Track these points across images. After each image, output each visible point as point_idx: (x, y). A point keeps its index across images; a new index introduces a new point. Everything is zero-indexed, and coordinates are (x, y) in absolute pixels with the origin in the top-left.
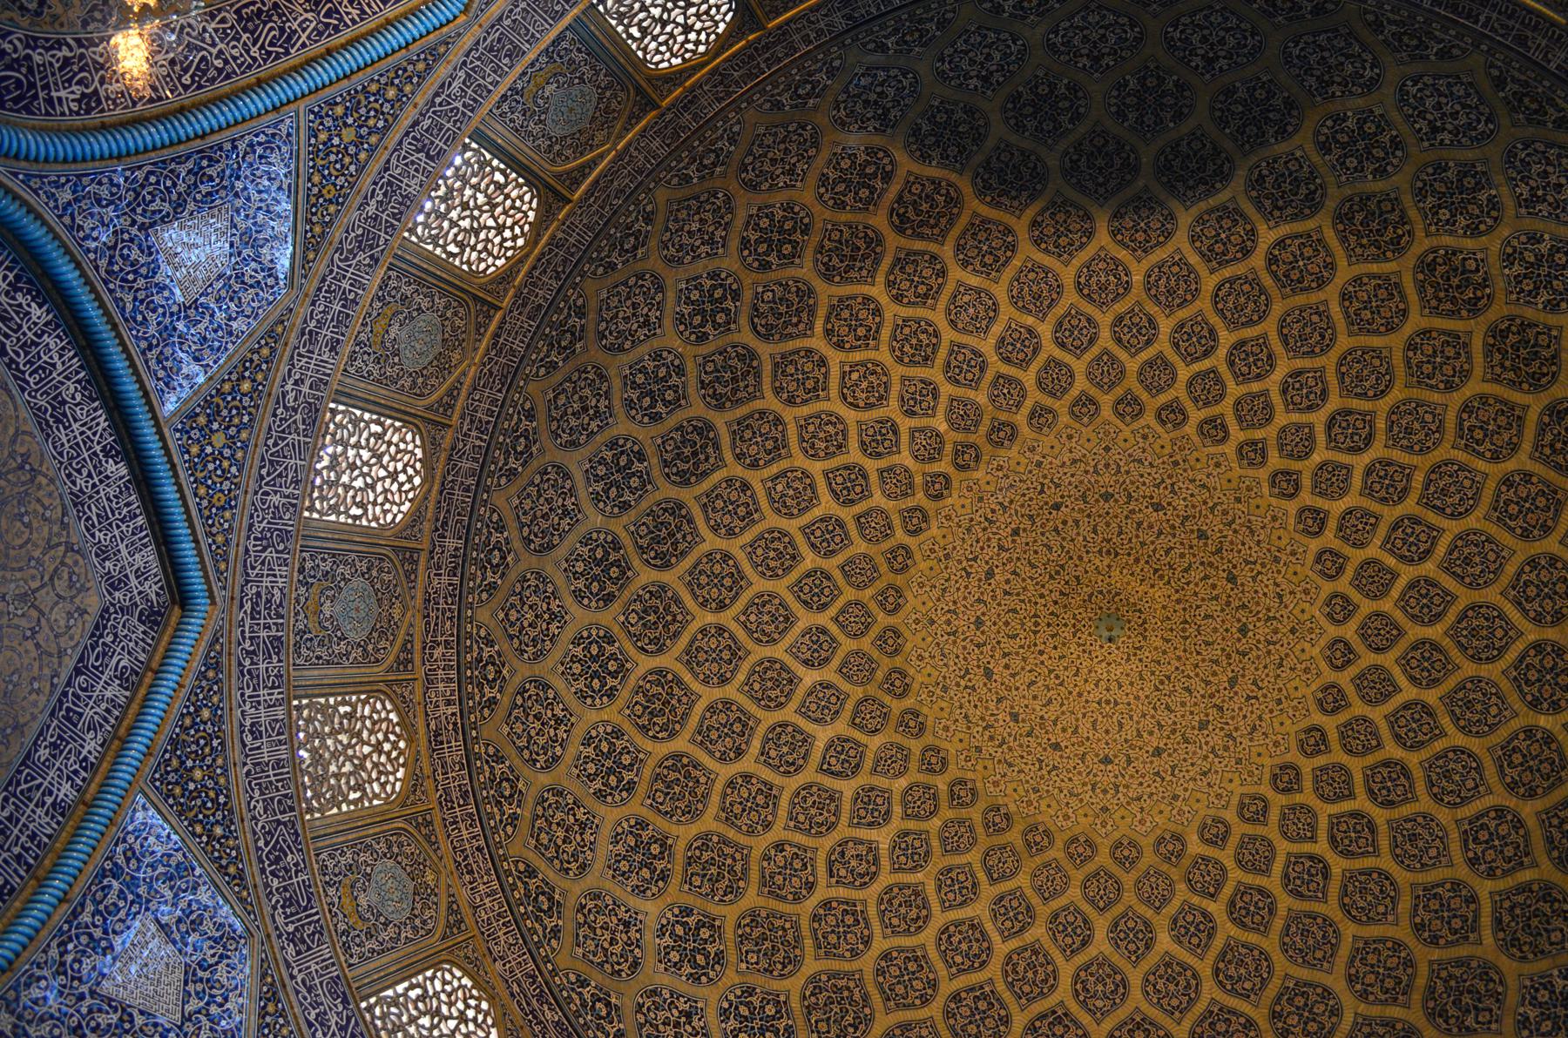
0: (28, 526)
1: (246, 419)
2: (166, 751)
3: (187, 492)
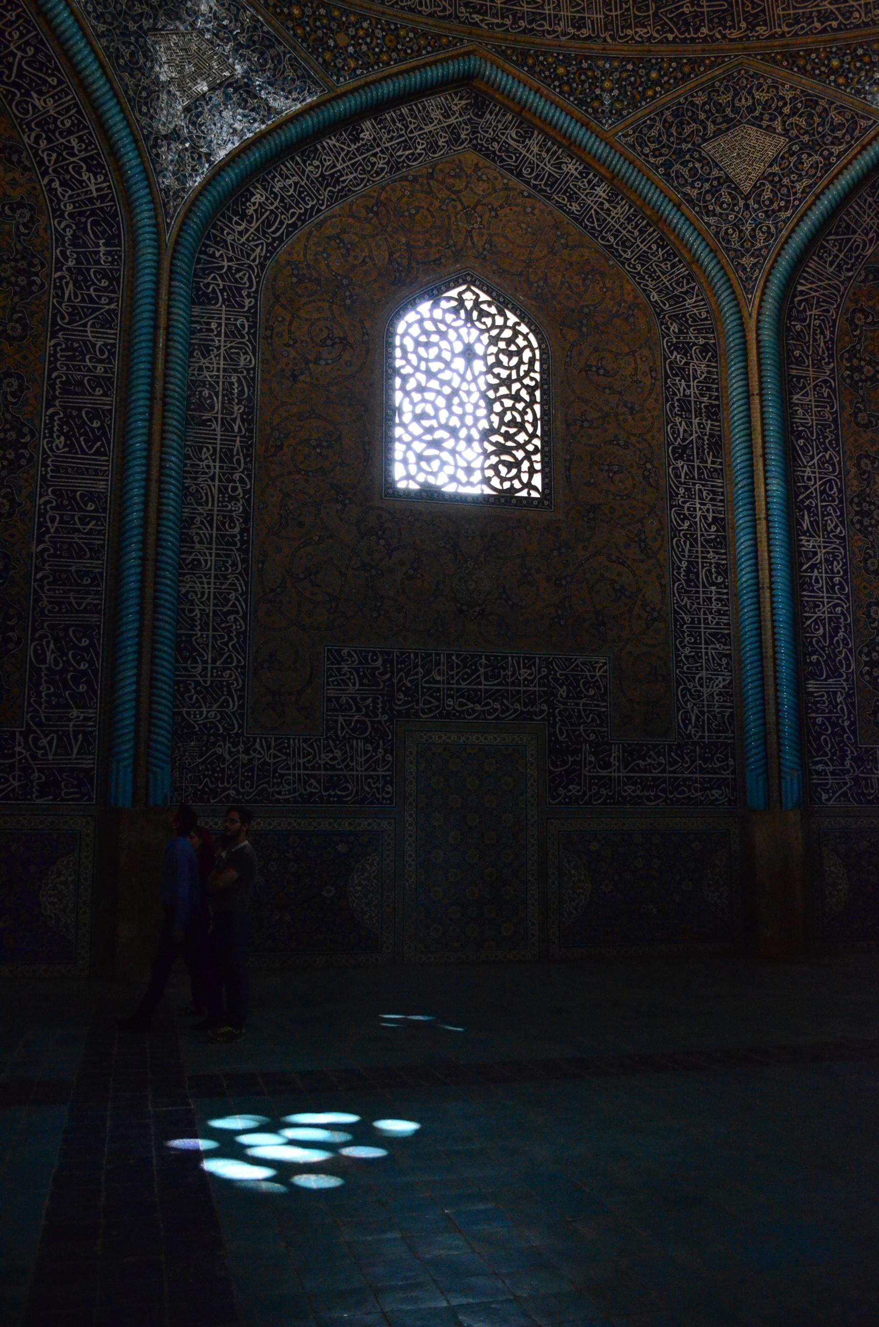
0: (418, 209)
1: (322, 11)
2: (586, 111)
3: (386, 73)
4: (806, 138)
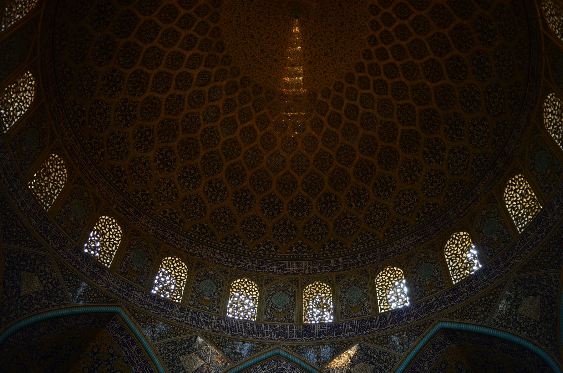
4: (48, 293)
